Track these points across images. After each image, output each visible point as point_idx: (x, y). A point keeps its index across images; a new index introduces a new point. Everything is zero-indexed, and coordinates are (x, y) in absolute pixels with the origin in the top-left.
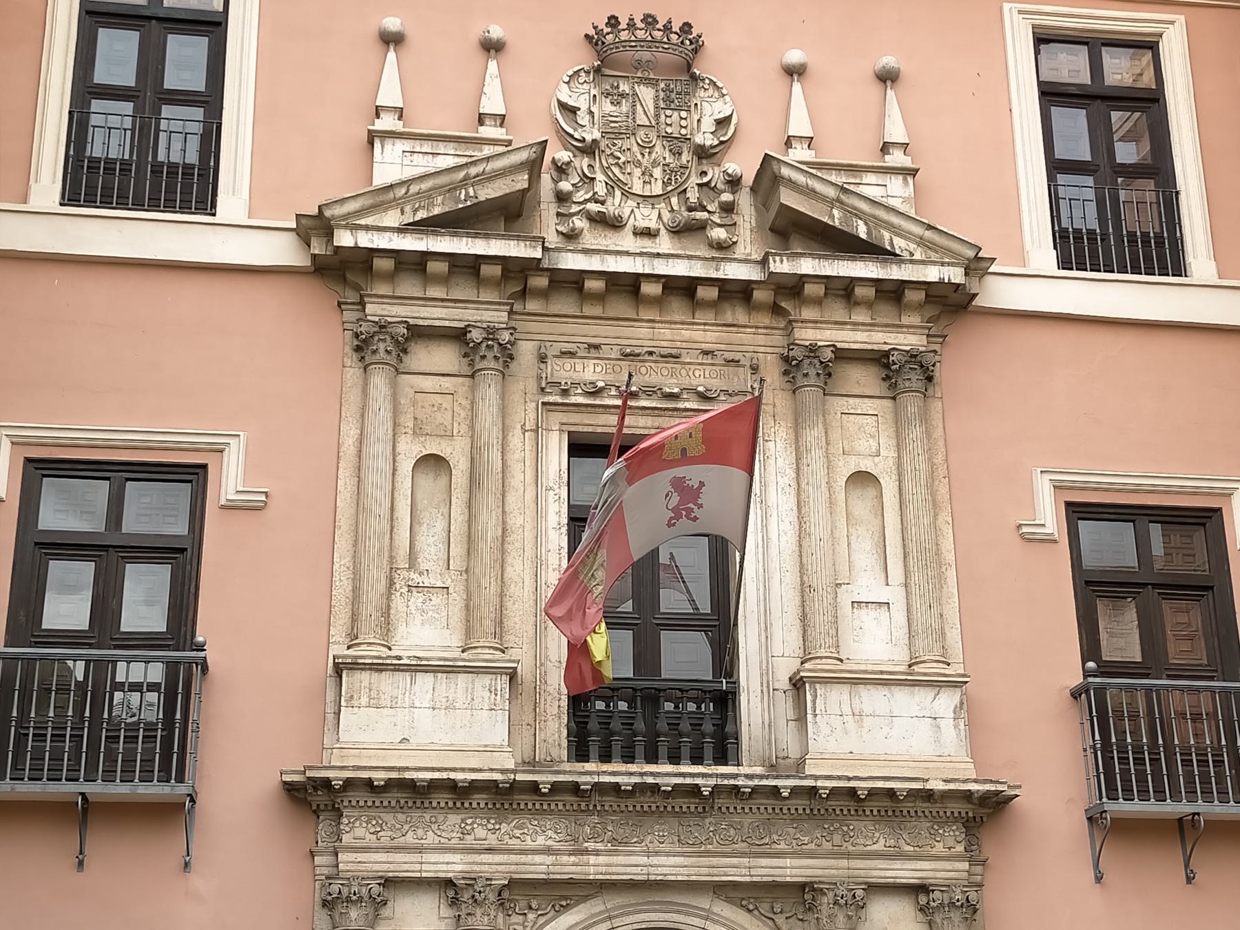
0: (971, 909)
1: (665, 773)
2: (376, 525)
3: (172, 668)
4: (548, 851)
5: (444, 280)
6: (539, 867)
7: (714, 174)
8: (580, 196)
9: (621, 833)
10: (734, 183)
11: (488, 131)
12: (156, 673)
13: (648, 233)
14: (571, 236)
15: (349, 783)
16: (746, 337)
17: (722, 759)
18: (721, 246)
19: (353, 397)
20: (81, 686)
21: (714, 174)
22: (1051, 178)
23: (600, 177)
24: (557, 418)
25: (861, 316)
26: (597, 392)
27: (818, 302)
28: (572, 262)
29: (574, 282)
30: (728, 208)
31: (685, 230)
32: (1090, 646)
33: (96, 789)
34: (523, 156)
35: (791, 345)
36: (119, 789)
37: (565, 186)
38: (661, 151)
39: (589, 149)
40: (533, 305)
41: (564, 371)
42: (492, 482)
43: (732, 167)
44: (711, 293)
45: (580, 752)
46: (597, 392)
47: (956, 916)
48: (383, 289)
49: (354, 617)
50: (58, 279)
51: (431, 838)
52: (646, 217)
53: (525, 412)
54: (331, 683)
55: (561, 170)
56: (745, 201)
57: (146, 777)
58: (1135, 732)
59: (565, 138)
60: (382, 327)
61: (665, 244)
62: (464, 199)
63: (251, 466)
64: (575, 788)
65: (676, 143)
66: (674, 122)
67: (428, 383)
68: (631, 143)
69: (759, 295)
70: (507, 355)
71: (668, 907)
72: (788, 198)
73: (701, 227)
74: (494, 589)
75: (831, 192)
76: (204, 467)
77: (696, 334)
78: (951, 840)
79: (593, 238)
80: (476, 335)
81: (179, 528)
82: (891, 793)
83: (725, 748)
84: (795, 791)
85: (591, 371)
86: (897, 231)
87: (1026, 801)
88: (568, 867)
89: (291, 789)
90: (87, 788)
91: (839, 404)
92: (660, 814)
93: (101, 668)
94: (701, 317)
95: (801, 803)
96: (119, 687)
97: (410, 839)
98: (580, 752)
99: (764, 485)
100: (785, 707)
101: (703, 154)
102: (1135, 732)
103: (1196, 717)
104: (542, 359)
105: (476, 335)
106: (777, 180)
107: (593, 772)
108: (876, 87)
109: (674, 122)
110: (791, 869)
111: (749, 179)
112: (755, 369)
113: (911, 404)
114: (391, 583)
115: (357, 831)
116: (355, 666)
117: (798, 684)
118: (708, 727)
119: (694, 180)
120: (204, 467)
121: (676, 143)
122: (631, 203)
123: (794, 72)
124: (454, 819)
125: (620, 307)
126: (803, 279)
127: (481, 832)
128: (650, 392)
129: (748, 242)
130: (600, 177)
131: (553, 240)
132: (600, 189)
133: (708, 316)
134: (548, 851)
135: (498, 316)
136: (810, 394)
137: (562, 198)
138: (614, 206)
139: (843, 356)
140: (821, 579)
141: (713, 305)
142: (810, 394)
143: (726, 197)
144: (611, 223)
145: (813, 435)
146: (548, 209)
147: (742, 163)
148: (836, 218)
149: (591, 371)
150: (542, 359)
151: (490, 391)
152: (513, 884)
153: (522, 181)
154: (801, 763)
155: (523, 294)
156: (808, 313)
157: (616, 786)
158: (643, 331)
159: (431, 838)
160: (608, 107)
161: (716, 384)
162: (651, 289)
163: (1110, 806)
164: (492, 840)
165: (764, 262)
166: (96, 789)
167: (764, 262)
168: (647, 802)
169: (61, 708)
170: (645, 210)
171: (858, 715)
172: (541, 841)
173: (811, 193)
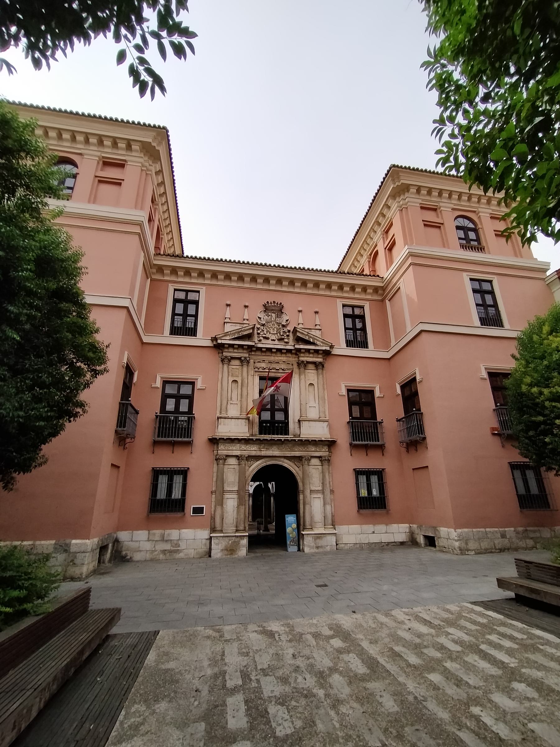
0: (329, 461)
1: (276, 437)
2: (225, 393)
3: (189, 418)
4: (255, 451)
5: (237, 349)
6: (253, 453)
7: (285, 330)
8: (261, 333)
9: (268, 447)
10: (289, 331)
11: (245, 322)
12: (186, 419)
13: (272, 340)
14: (260, 341)
15: (220, 438)
16: (291, 359)
17: (286, 435)
18: (286, 343)
19: (221, 370)
20: (173, 421)
21: (285, 330)
22: (345, 331)
23: (265, 330)
24: (257, 373)
25: (311, 355)
26: (264, 369)
27: (304, 353)
28: (260, 345)
29: (260, 349)
30: (288, 336)
31: (280, 340)
32: (351, 414)
33: (176, 439)
34: (252, 326)
35: (299, 360)
36: (180, 439)
37: (259, 332)
38: (276, 326)
39: (263, 325)
40: (253, 353)
41: (258, 365)
42: (245, 385)
43: (289, 328)
44: (285, 351)
45: (260, 433)
46: (264, 369)
47: (326, 462)
48: (226, 350)
49: (221, 409)
50: (168, 348)
51: (234, 448)
52: (273, 337)
53: (252, 372)
54: (217, 421)
55: (258, 329)
56: (291, 334)
57: (184, 437)
58: (358, 430)
59: (259, 323)
60: (226, 357)
61: (276, 342)
62: (241, 334)
63: (203, 382)
64: (259, 439)
65: (279, 324)
66: (278, 320)
67: (234, 367)
68: (270, 324)
69: (293, 351)
70: (248, 362)
71: (276, 460)
72: (298, 334)
73: (283, 339)
74: (246, 404)
75: (306, 333)
76: (194, 382)
77: (282, 358)
78: (326, 448)
79: (264, 341)
80: (243, 359)
81: (190, 392)
82: (315, 440)
83: (287, 433)
84: (298, 440)
85: (263, 365)
86: (318, 340)
87: (339, 441)
88: (258, 453)
89: (209, 439)
90: (174, 439)
91: (307, 371)
92: (275, 444)
93: (176, 418)
94: (283, 355)
95: (299, 442)
96: (180, 421)
97: (231, 448)
98: (260, 433)
99: (294, 386)
100: (297, 425)
101: (283, 326)
102: (358, 430)
103: (369, 427)
104: (255, 363)
105: (243, 359)
106: (297, 331)
107: (263, 437)
108: (314, 314)
109: (278, 320)
110: (297, 454)
111: (292, 331)
112: (292, 365)
113: (320, 371)
114: (227, 403)
115: (221, 447)
116: (221, 418)
117: (299, 421)
118: (283, 429)
119: (282, 331)
120: (194, 382)
121: (279, 324)
122: (271, 335)
123: (300, 311)
124: (238, 445)
125: (268, 354)
126: (301, 349)
127: (243, 447)
128: (274, 369)
129: (291, 342)
130: (265, 330)
131: (257, 342)
132: (265, 332)
133: (284, 355)
134: (255, 451)
135: (247, 355)
136: (302, 369)
137: (258, 334)
138: (267, 336)
139: (308, 363)
140: (303, 403)
141: (285, 353)
142: (302, 369)
143: (288, 334)
144: (267, 338)
145: (303, 377)
146: (256, 335)
147: (290, 328)
148: (307, 338)
149: (263, 365)
150: (255, 363)
151: (245, 369)
152: (249, 456)
153: (251, 331)
154: (300, 435)
155: (251, 351)
156: (302, 355)
157: (267, 439)
158: (272, 358)
159: (234, 448)
160: (266, 317)
161: (285, 367)
162: (273, 350)
163: (353, 443)
164: (245, 449)
165: (294, 346)
166: (176, 439)
167: (294, 346)
168: (273, 442)
169: (169, 425)
170: (273, 336)
171: (310, 427)
172: (254, 449)
173: (303, 334)
